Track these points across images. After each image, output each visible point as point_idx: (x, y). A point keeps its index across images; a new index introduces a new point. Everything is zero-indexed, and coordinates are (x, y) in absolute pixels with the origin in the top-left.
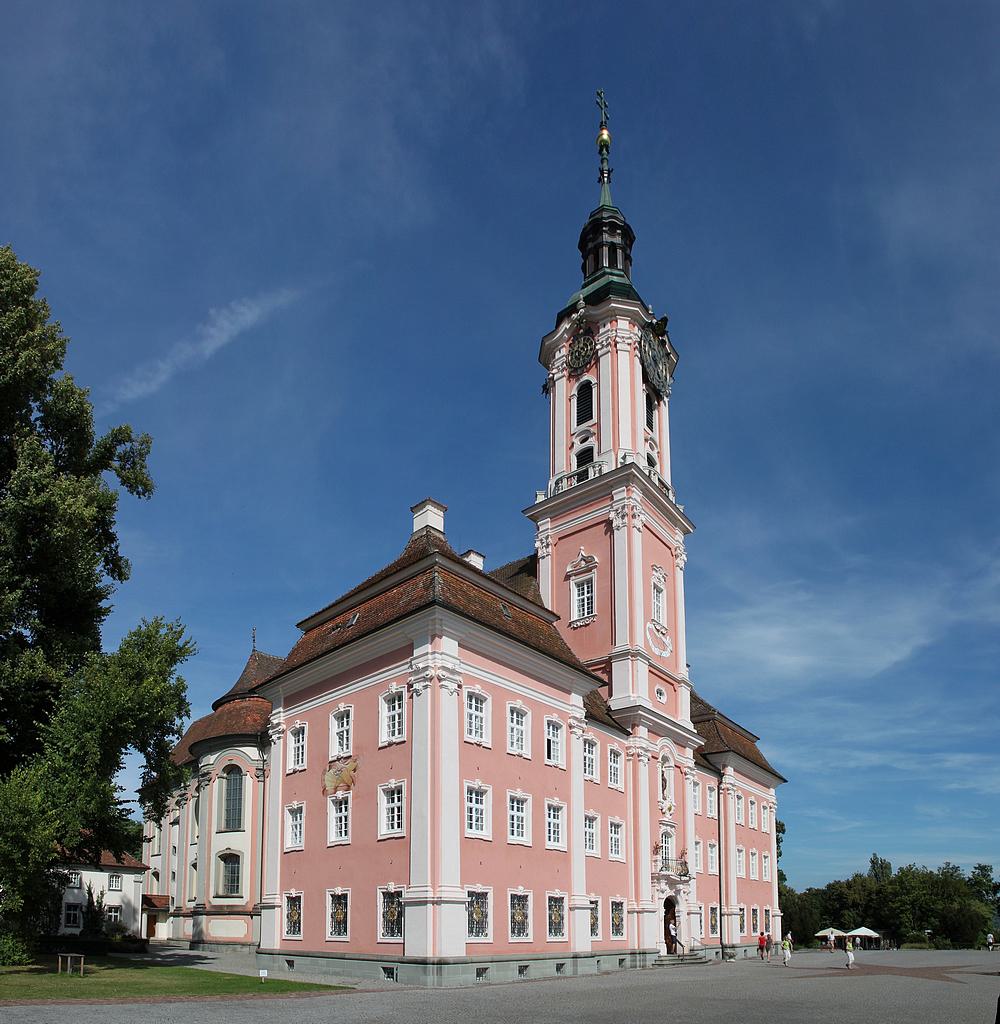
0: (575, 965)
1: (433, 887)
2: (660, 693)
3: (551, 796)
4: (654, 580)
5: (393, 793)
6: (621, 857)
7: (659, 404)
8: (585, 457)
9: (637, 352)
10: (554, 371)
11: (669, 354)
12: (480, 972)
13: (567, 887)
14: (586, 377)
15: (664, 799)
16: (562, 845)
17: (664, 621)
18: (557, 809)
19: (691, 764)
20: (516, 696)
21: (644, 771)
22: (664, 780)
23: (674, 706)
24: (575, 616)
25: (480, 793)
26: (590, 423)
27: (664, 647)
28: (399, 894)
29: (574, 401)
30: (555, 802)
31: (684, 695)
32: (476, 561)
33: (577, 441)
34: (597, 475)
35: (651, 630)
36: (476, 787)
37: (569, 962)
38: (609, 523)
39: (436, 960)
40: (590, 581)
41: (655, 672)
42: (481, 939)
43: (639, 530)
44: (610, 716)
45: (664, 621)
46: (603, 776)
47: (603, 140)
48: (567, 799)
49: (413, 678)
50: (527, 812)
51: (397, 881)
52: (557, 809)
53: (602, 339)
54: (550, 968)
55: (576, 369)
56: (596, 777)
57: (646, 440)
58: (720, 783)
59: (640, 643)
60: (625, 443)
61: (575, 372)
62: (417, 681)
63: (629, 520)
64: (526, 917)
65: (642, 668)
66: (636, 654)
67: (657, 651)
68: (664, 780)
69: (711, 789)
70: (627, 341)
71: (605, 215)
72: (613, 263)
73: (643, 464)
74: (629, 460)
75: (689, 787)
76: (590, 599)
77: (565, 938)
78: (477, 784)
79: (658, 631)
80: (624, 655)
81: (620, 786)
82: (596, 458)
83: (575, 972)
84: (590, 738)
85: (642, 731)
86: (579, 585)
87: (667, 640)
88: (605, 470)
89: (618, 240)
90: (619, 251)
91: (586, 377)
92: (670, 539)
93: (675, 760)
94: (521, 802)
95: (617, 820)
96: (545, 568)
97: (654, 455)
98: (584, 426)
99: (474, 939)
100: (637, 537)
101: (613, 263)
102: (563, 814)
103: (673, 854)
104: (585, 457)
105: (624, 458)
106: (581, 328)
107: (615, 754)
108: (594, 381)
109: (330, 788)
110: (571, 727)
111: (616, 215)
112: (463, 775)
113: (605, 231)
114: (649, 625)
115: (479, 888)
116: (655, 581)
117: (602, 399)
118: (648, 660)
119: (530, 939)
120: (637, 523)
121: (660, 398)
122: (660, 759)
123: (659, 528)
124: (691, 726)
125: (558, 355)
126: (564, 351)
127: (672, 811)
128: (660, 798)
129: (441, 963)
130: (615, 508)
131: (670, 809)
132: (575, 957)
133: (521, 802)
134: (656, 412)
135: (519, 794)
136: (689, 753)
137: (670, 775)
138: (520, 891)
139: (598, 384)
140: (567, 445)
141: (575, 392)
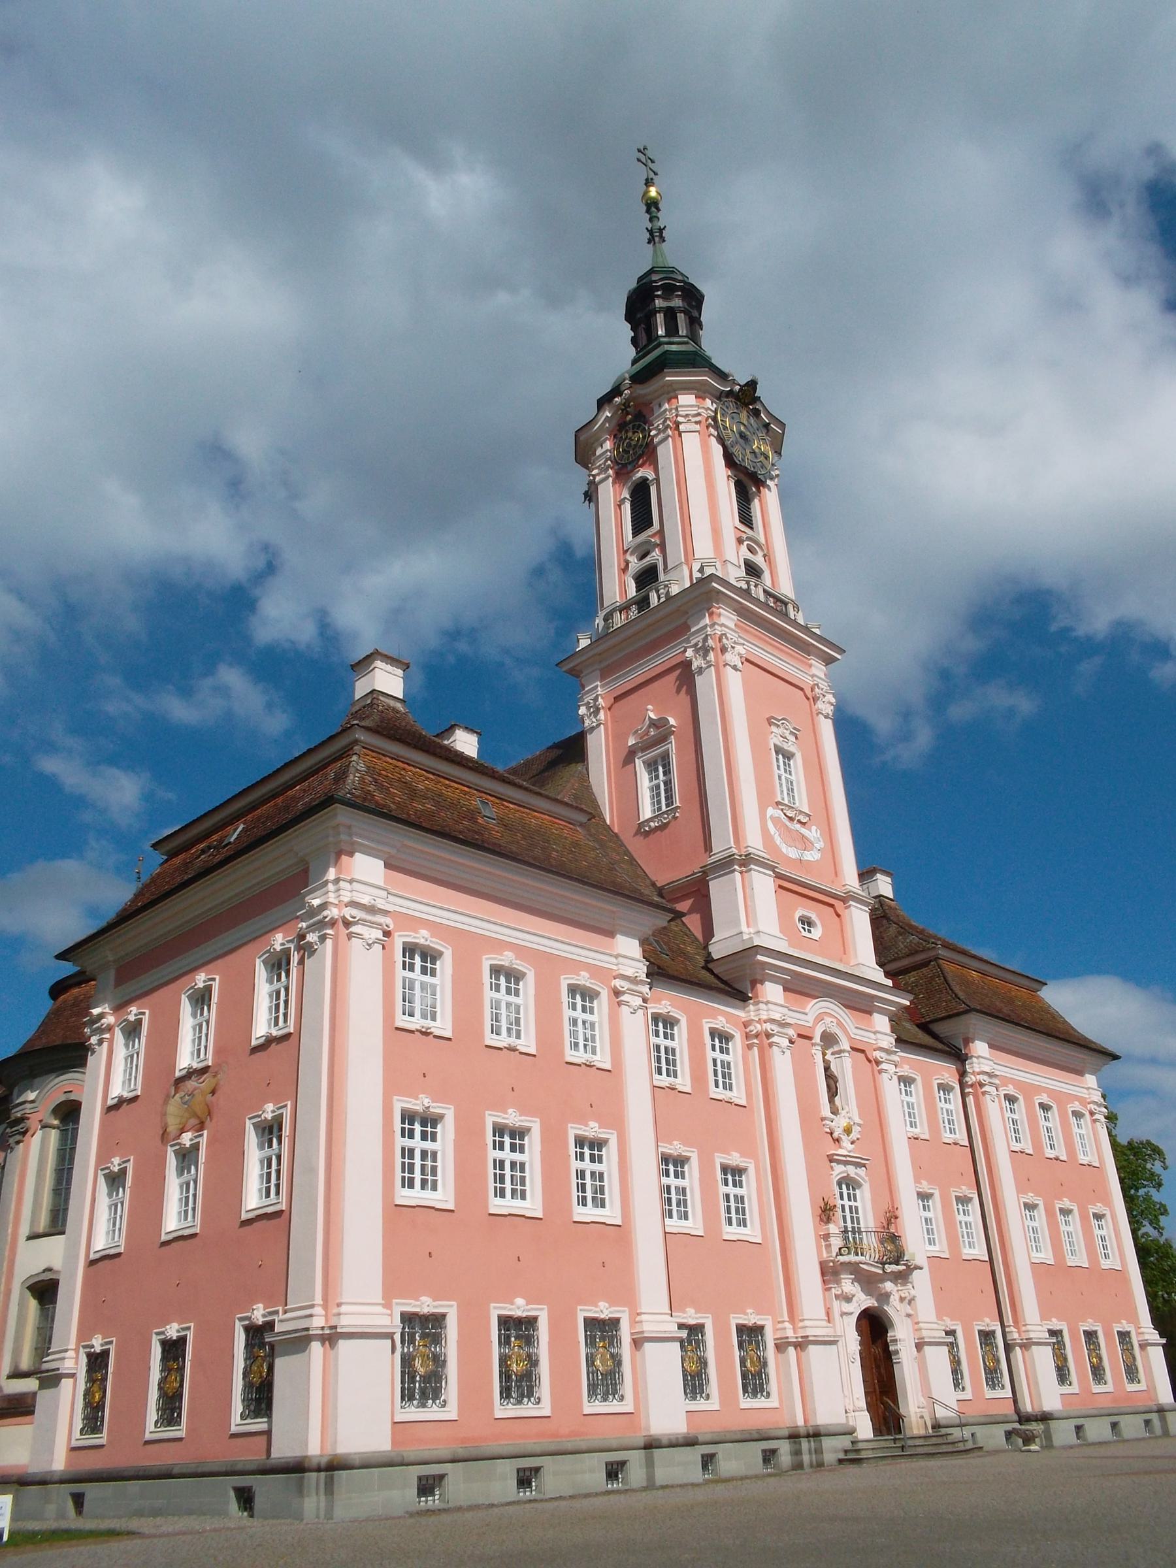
0: (650, 1464)
1: (325, 1306)
2: (807, 922)
3: (583, 1120)
4: (774, 740)
5: (270, 1131)
6: (751, 1232)
7: (759, 491)
8: (647, 577)
9: (712, 430)
10: (595, 472)
11: (769, 424)
12: (426, 1487)
13: (627, 1294)
14: (641, 473)
15: (835, 1112)
16: (611, 1214)
17: (802, 803)
18: (597, 1144)
19: (888, 1041)
20: (500, 945)
21: (783, 1064)
22: (831, 1078)
23: (844, 946)
24: (647, 812)
25: (430, 1121)
26: (650, 531)
27: (806, 844)
28: (270, 1326)
29: (627, 506)
30: (592, 1129)
31: (860, 921)
32: (466, 743)
33: (633, 560)
34: (662, 600)
35: (775, 820)
36: (420, 1108)
37: (635, 1459)
38: (687, 664)
39: (324, 1461)
40: (665, 759)
41: (788, 885)
42: (432, 1412)
43: (735, 668)
44: (711, 971)
45: (802, 803)
46: (698, 1077)
47: (651, 198)
48: (617, 1121)
49: (304, 925)
50: (532, 1154)
51: (269, 1300)
52: (597, 1144)
53: (658, 423)
54: (592, 1472)
55: (624, 466)
56: (684, 1082)
57: (740, 541)
58: (962, 1074)
59: (754, 842)
60: (703, 548)
61: (623, 469)
62: (311, 929)
63: (716, 657)
64: (533, 1361)
65: (763, 884)
66: (747, 861)
67: (793, 853)
68: (831, 1078)
69: (945, 1088)
70: (694, 419)
71: (655, 277)
72: (672, 330)
73: (735, 574)
74: (708, 571)
75: (890, 1088)
76: (668, 784)
77: (627, 1406)
78: (420, 1103)
79: (791, 819)
80: (726, 865)
81: (738, 1095)
82: (662, 576)
83: (651, 1477)
84: (663, 1011)
85: (772, 991)
86: (651, 766)
87: (813, 833)
88: (675, 590)
89: (677, 302)
90: (681, 317)
91: (641, 473)
92: (799, 675)
93: (850, 1038)
94: (518, 1134)
95: (735, 1159)
96: (599, 747)
97: (759, 560)
98: (642, 537)
99: (413, 1413)
100: (734, 682)
101: (672, 330)
102: (611, 1153)
103: (868, 1220)
104: (647, 577)
105: (701, 570)
106: (628, 414)
107: (722, 1037)
108: (651, 475)
109: (172, 1129)
110: (617, 993)
111: (671, 275)
112: (391, 1088)
113: (658, 296)
114: (771, 811)
115: (425, 1305)
116: (778, 741)
117: (665, 498)
118: (773, 868)
119: (545, 1409)
120: (731, 658)
121: (759, 483)
122: (817, 1039)
123: (777, 662)
124: (878, 975)
125: (599, 452)
126: (608, 445)
127: (854, 1135)
128: (826, 1111)
129: (334, 1466)
130: (693, 642)
131: (848, 1131)
132: (651, 1445)
133: (518, 1134)
134: (756, 505)
135: (512, 1118)
136: (881, 1023)
137: (845, 1068)
138: (519, 1308)
139: (657, 480)
140: (619, 565)
141: (626, 494)
